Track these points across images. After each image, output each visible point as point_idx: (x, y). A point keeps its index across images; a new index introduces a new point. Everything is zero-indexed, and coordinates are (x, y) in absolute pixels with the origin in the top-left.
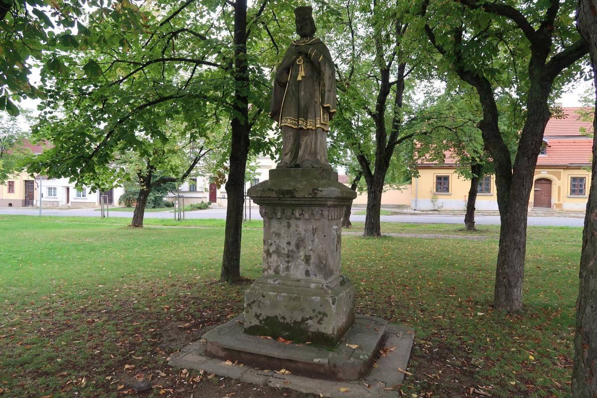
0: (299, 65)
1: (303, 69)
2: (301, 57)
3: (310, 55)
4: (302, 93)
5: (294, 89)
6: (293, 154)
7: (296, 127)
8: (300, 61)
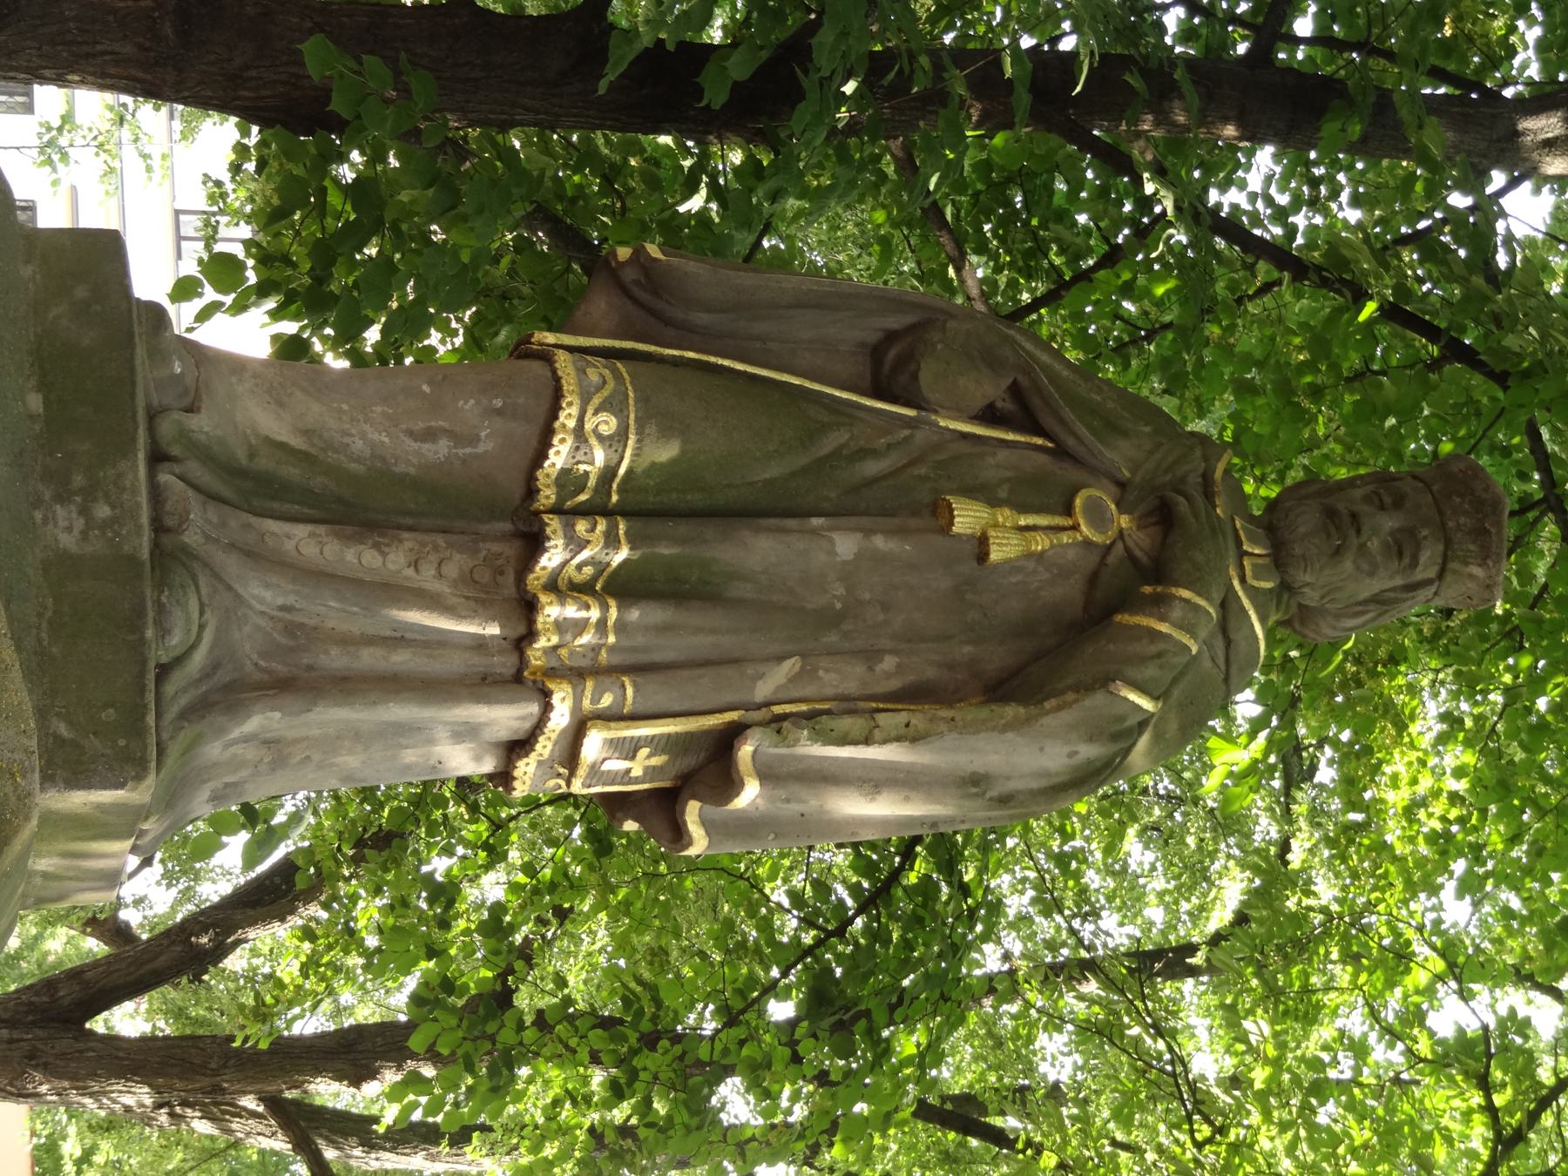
0: (1068, 511)
1: (1040, 543)
2: (1124, 521)
3: (1159, 604)
4: (846, 545)
5: (872, 468)
6: (291, 472)
7: (548, 495)
8: (1097, 515)
